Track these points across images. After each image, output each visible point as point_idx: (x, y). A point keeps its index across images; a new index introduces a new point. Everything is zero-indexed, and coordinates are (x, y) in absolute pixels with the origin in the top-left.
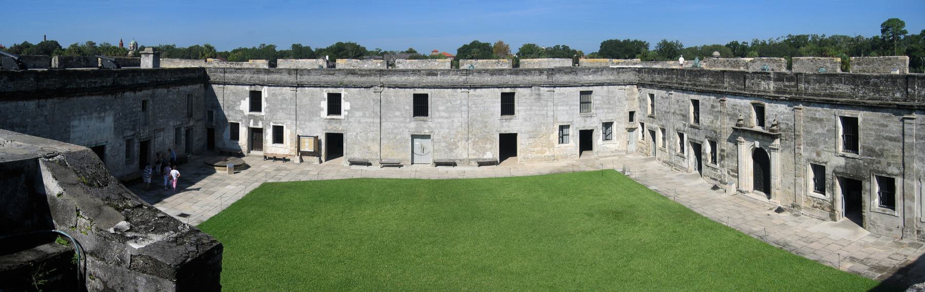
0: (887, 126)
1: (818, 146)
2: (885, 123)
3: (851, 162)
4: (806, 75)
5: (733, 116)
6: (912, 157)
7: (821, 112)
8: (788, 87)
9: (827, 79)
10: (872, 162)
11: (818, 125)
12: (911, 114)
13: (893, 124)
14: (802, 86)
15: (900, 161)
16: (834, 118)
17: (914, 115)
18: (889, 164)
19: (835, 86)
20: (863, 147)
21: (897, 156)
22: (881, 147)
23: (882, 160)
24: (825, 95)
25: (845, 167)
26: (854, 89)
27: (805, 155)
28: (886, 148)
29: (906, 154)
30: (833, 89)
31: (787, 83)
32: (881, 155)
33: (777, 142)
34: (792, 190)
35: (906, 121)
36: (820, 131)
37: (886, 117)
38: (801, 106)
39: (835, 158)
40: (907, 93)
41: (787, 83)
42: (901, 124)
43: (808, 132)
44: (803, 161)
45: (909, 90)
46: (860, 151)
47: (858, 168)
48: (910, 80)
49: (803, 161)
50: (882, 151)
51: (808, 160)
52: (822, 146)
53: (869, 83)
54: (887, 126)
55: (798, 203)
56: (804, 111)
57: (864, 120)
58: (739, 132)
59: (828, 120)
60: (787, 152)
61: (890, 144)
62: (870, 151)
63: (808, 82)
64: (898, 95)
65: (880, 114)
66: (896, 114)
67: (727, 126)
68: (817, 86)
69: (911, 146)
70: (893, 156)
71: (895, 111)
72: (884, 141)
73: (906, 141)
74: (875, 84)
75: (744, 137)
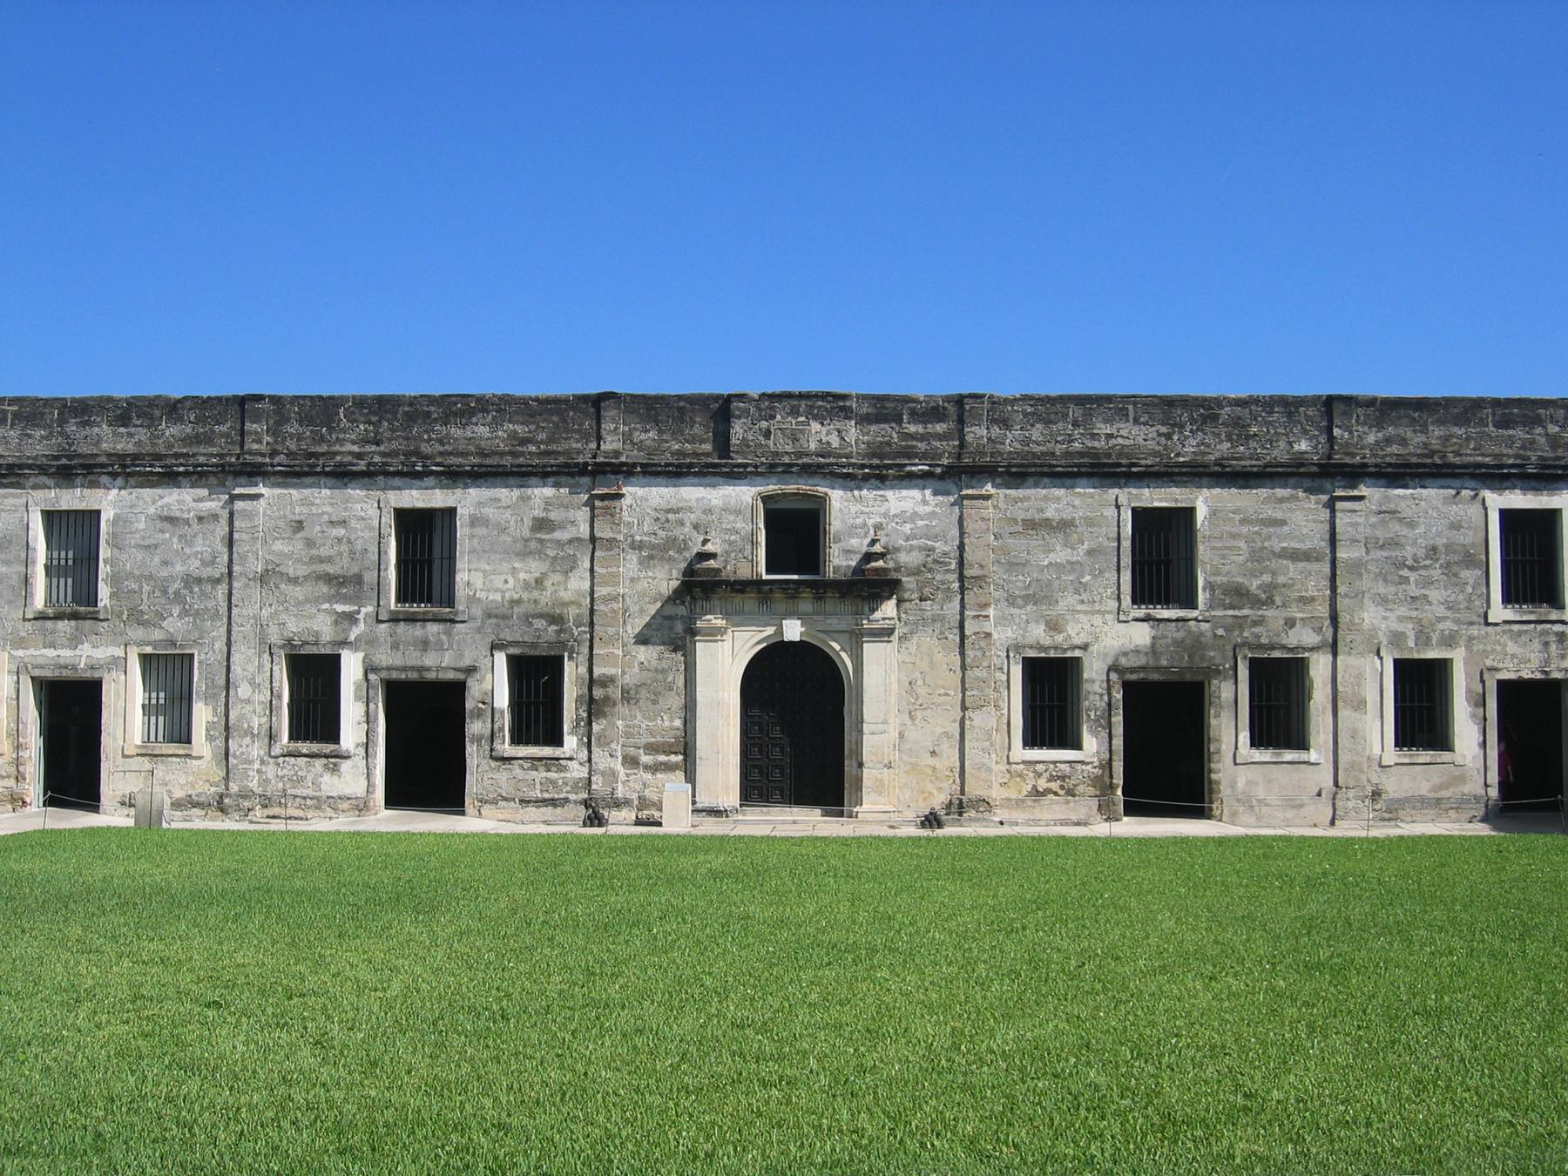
0: (1283, 523)
1: (1051, 601)
2: (1279, 515)
3: (1172, 632)
4: (995, 402)
5: (652, 553)
6: (1359, 595)
7: (1057, 501)
8: (923, 438)
9: (1074, 411)
10: (1240, 623)
11: (1056, 541)
12: (1354, 487)
13: (1302, 515)
14: (977, 433)
15: (1323, 610)
16: (1106, 513)
17: (1363, 490)
18: (1290, 623)
19: (1103, 429)
20: (1211, 586)
21: (1313, 599)
22: (1267, 578)
23: (1269, 613)
24: (1067, 454)
25: (1153, 650)
26: (1168, 436)
27: (1003, 635)
28: (1281, 579)
29: (1341, 589)
30: (1094, 436)
31: (912, 428)
32: (1269, 601)
33: (889, 608)
34: (951, 756)
35: (1339, 505)
36: (1060, 555)
37: (1281, 500)
38: (989, 488)
39: (1112, 635)
40: (1331, 439)
41: (912, 428)
42: (1326, 514)
43: (1013, 566)
44: (997, 656)
45: (1336, 432)
46: (1202, 597)
47: (1195, 645)
48: (1338, 408)
49: (997, 656)
50: (1270, 588)
51: (1018, 648)
52: (1068, 600)
53: (1215, 418)
54: (1283, 523)
55: (974, 790)
56: (998, 504)
57: (1213, 513)
58: (702, 587)
59: (1090, 522)
60: (926, 639)
61: (1293, 570)
62: (1237, 595)
63: (1005, 423)
64: (1303, 446)
65: (1263, 492)
66: (1310, 491)
67: (646, 586)
68: (1037, 432)
69: (1357, 567)
70: (1301, 599)
71: (1308, 483)
72: (1274, 563)
73: (1341, 554)
74: (1236, 422)
75: (727, 615)
